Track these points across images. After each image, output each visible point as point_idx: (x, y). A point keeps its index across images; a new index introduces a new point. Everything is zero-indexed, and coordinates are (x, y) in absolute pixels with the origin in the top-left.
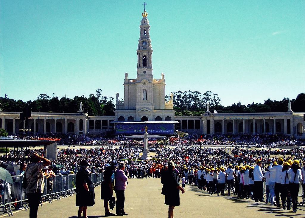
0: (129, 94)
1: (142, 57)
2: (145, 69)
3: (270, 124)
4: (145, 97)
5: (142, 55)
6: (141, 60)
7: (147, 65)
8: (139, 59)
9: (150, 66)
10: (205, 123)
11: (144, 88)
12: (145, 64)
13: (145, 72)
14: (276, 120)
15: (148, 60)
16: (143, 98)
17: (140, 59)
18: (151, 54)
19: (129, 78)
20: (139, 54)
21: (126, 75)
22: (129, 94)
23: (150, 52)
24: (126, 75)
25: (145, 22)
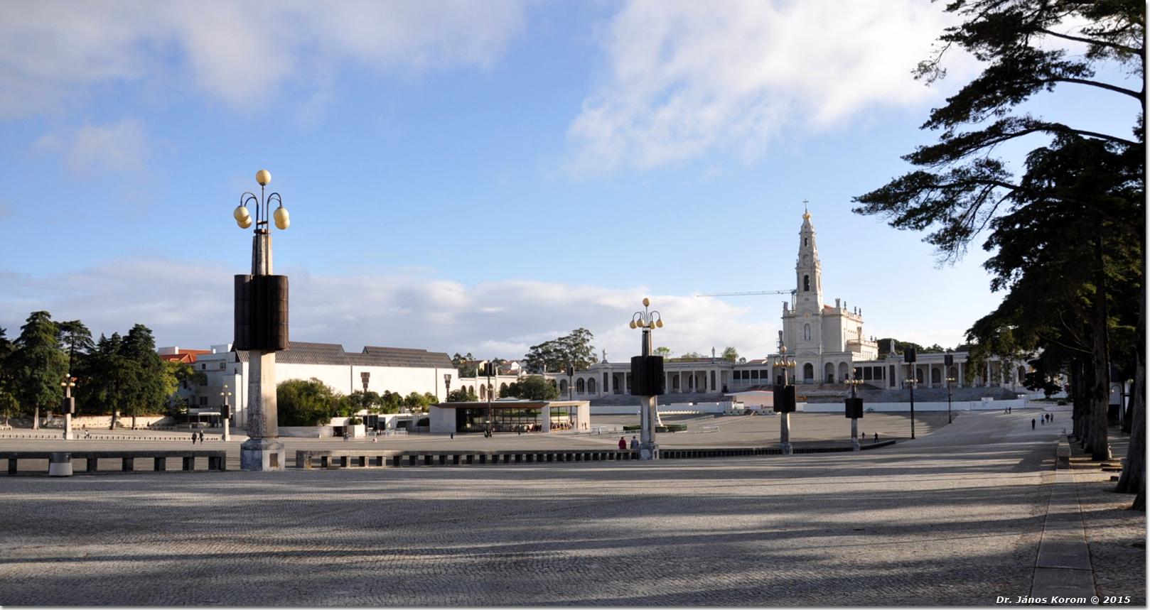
1: (802, 278)
3: (924, 372)
4: (807, 335)
9: (814, 290)
10: (888, 370)
11: (805, 323)
12: (807, 288)
13: (807, 299)
14: (933, 365)
20: (798, 273)
25: (806, 227)
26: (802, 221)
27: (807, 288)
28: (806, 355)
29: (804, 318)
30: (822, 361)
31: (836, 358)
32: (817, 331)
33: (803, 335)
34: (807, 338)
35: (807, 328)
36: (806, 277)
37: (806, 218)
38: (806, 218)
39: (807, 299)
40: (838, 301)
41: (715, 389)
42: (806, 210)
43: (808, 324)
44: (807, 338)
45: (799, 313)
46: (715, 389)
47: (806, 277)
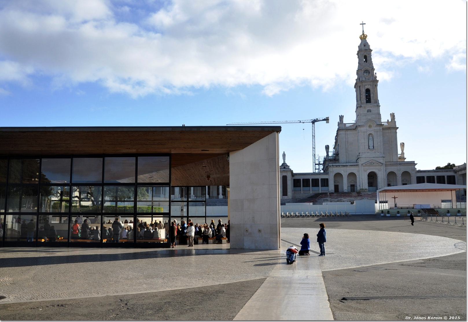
0: (347, 143)
2: (369, 106)
5: (364, 88)
6: (362, 95)
7: (372, 100)
8: (360, 94)
9: (377, 102)
11: (369, 133)
13: (369, 111)
15: (373, 94)
16: (369, 146)
17: (361, 94)
18: (376, 86)
19: (345, 121)
21: (341, 118)
22: (347, 143)
23: (375, 81)
24: (341, 118)
25: (365, 46)
26: (359, 42)
27: (368, 100)
28: (371, 163)
29: (368, 128)
30: (386, 171)
31: (399, 167)
32: (378, 141)
33: (367, 144)
34: (371, 147)
35: (371, 138)
36: (368, 91)
37: (363, 38)
38: (363, 38)
39: (369, 111)
40: (393, 116)
41: (286, 195)
42: (363, 31)
43: (370, 134)
44: (371, 147)
45: (362, 124)
46: (286, 195)
47: (368, 91)
